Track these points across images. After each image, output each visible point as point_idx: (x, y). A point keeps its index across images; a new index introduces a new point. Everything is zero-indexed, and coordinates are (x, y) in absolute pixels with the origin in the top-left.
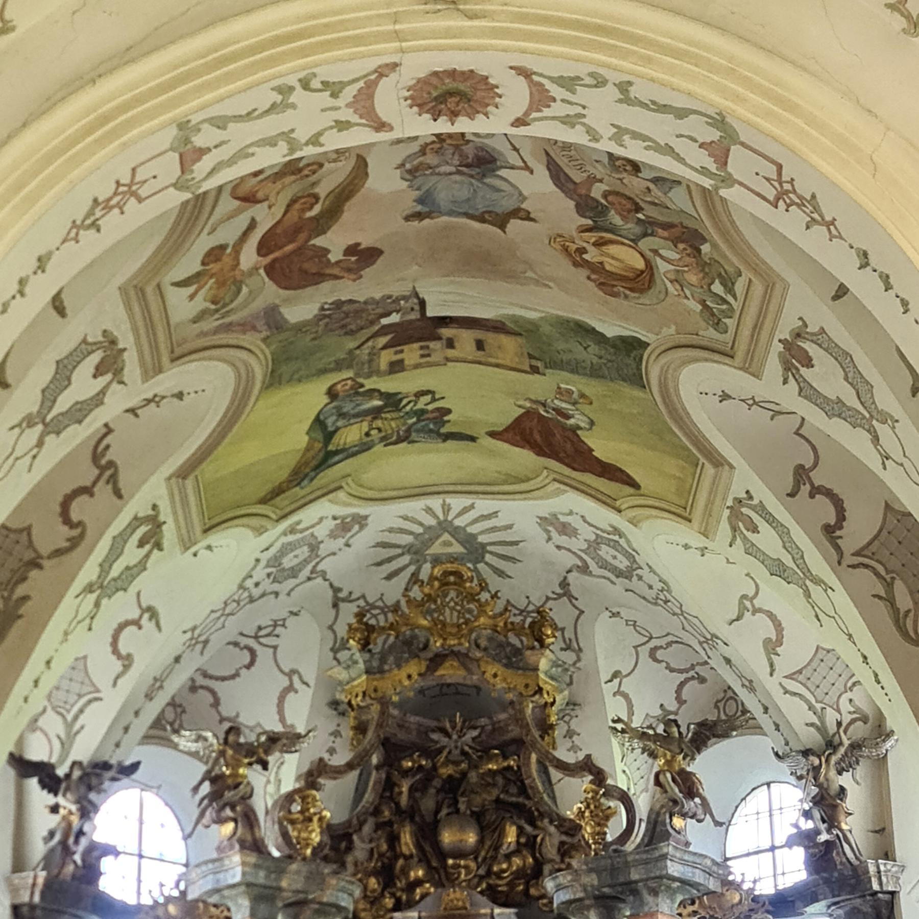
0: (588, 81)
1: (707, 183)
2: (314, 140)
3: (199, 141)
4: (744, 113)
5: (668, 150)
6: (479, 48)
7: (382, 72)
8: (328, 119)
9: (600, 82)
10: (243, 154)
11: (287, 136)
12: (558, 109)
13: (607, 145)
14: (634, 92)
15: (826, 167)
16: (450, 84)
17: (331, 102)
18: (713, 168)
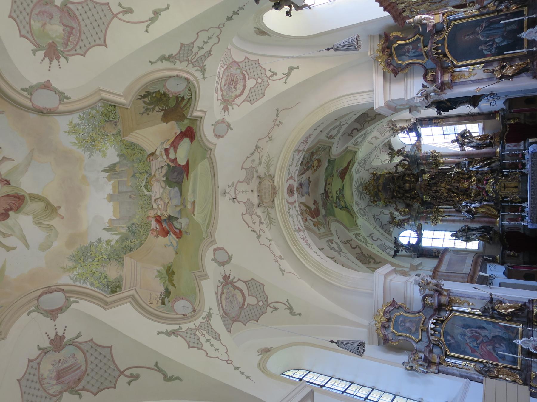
1: (304, 153)
2: (297, 211)
3: (297, 229)
4: (294, 148)
5: (299, 159)
7: (287, 201)
8: (294, 209)
9: (289, 169)
10: (299, 222)
13: (298, 167)
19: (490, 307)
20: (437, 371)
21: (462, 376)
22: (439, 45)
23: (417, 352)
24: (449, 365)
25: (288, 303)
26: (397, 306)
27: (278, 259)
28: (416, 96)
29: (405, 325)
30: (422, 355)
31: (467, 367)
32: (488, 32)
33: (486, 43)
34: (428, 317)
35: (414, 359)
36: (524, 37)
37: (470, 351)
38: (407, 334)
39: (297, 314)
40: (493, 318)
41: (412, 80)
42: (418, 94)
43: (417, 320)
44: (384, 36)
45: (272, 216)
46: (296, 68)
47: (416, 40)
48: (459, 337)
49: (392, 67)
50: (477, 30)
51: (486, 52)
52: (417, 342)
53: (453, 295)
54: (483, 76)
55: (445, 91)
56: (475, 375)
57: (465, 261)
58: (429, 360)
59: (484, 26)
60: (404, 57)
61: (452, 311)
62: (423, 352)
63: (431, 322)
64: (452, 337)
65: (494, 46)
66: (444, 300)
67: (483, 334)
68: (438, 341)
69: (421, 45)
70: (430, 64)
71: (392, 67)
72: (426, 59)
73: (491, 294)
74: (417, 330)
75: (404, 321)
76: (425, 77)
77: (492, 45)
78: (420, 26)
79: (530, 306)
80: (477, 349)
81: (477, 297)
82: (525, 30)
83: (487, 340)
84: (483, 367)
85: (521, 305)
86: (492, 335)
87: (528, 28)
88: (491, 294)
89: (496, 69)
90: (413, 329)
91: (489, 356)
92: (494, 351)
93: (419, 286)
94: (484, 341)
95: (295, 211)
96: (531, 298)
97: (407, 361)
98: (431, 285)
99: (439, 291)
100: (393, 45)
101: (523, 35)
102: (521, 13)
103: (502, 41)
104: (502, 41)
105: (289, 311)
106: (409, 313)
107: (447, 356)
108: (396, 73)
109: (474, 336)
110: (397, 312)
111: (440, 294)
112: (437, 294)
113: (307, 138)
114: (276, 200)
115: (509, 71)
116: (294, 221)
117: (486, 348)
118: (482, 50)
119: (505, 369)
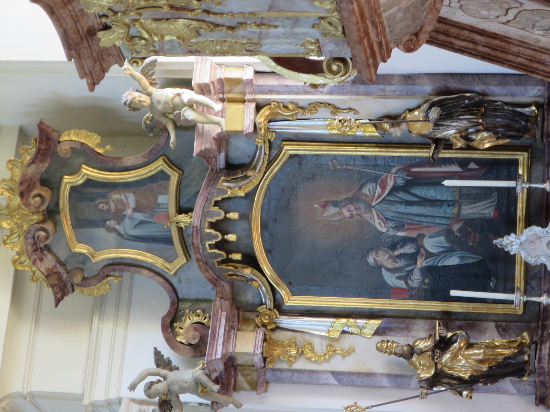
22: (234, 215)
32: (402, 209)
33: (393, 247)
42: (133, 387)
44: (35, 133)
47: (153, 179)
49: (49, 262)
50: (365, 190)
51: (391, 279)
55: (238, 396)
59: (390, 184)
60: (101, 232)
65: (421, 262)
69: (168, 200)
70: (195, 282)
71: (49, 262)
72: (181, 260)
76: (170, 325)
77: (412, 258)
82: (520, 225)
87: (528, 223)
89: (421, 345)
101: (511, 243)
102: (508, 169)
103: (448, 251)
104: (448, 251)
108: (62, 290)
115: (463, 362)
118: (379, 267)
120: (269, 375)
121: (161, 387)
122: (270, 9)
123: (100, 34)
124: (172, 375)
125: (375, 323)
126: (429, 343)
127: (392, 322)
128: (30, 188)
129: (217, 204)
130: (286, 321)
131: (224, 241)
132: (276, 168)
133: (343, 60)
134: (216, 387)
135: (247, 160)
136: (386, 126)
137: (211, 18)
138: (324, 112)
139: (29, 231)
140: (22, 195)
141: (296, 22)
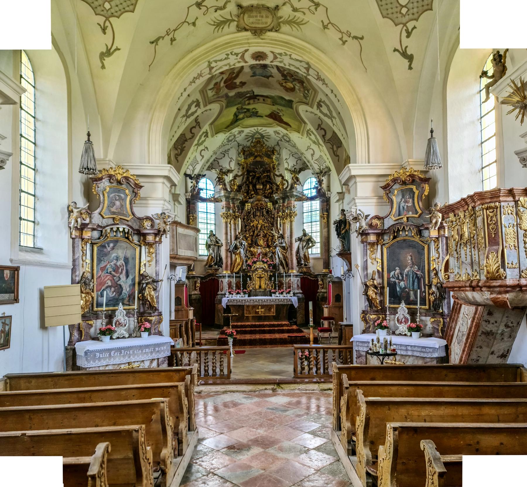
0: (284, 54)
1: (305, 75)
2: (234, 65)
3: (212, 65)
4: (312, 62)
5: (298, 68)
6: (264, 46)
7: (246, 51)
8: (236, 61)
9: (286, 55)
10: (221, 68)
11: (229, 64)
12: (279, 60)
13: (287, 67)
14: (292, 56)
15: (326, 74)
16: (259, 54)
17: (236, 58)
18: (306, 72)
19: (149, 280)
20: (73, 236)
21: (74, 261)
22: (407, 233)
23: (90, 215)
24: (83, 248)
25: (115, 50)
26: (136, 190)
27: (171, 36)
28: (358, 208)
29: (116, 200)
30: (87, 221)
31: (85, 265)
32: (411, 276)
33: (401, 274)
34: (130, 223)
35: (81, 214)
36: (401, 305)
37: (103, 265)
38: (106, 202)
39: (103, 63)
40: (139, 283)
41: (374, 204)
42: (359, 210)
43: (125, 213)
44: (427, 177)
45: (226, 27)
46: (410, 65)
47: (416, 210)
48: (114, 255)
51: (392, 273)
52: (100, 214)
53: (156, 246)
54: (370, 271)
55: (360, 235)
56: (79, 273)
57: (190, 250)
58: (84, 228)
59: (418, 273)
61: (140, 246)
62: (90, 221)
63: (125, 227)
64: (113, 248)
65: (397, 281)
66: (150, 238)
67: (121, 276)
68: (106, 236)
69: (410, 214)
70: (389, 223)
72: (394, 219)
73: (162, 280)
74: (114, 213)
75: (120, 199)
76: (377, 217)
77: (398, 279)
78: (430, 216)
79: (156, 314)
80: (105, 271)
81: (157, 268)
82: (408, 306)
83: (117, 280)
84: (88, 279)
85: (155, 307)
86: (122, 284)
88: (162, 280)
89: (375, 282)
90: (113, 209)
91: (101, 284)
92: (107, 287)
93: (161, 214)
94: (115, 278)
95: (234, 62)
96: (163, 313)
97: (77, 206)
98: (164, 225)
99: (158, 233)
100: (415, 187)
103: (400, 288)
104: (400, 288)
105: (104, 50)
106: (131, 204)
107: (92, 244)
108: (384, 188)
109: (118, 268)
110: (129, 191)
111: (156, 235)
112: (156, 232)
113: (323, 80)
114: (248, 33)
115: (371, 293)
116: (221, 60)
117: (108, 279)
118: (395, 270)
119: (91, 299)
120: (365, 244)
121: (360, 217)
122: (462, 262)
123: (453, 214)
124: (363, 220)
125: (380, 270)
126: (376, 284)
127: (381, 274)
128: (412, 177)
129: (410, 228)
130: (379, 247)
131: (400, 231)
132: (421, 243)
133: (449, 278)
134: (361, 232)
135: (422, 235)
136: (434, 272)
137: (459, 246)
138: (437, 256)
139: (399, 177)
140: (410, 175)
141: (459, 268)
